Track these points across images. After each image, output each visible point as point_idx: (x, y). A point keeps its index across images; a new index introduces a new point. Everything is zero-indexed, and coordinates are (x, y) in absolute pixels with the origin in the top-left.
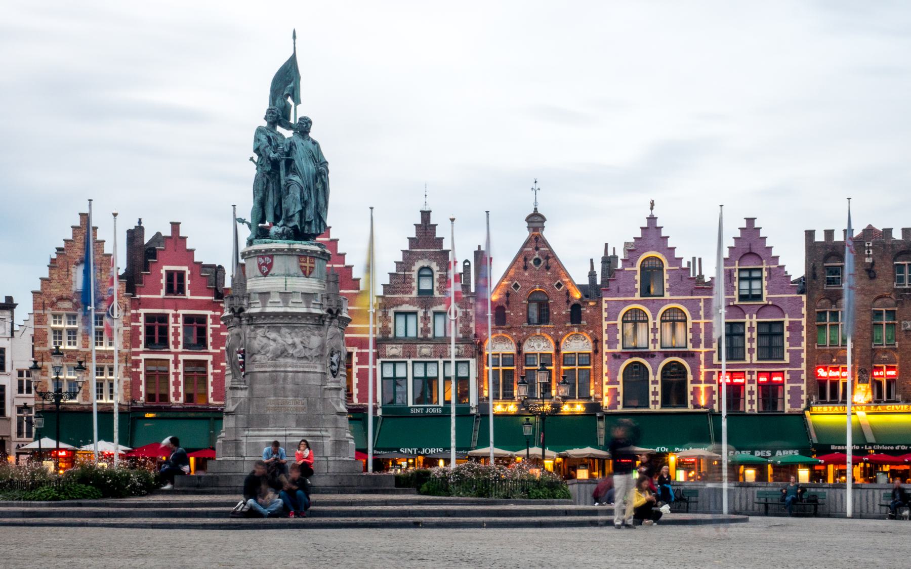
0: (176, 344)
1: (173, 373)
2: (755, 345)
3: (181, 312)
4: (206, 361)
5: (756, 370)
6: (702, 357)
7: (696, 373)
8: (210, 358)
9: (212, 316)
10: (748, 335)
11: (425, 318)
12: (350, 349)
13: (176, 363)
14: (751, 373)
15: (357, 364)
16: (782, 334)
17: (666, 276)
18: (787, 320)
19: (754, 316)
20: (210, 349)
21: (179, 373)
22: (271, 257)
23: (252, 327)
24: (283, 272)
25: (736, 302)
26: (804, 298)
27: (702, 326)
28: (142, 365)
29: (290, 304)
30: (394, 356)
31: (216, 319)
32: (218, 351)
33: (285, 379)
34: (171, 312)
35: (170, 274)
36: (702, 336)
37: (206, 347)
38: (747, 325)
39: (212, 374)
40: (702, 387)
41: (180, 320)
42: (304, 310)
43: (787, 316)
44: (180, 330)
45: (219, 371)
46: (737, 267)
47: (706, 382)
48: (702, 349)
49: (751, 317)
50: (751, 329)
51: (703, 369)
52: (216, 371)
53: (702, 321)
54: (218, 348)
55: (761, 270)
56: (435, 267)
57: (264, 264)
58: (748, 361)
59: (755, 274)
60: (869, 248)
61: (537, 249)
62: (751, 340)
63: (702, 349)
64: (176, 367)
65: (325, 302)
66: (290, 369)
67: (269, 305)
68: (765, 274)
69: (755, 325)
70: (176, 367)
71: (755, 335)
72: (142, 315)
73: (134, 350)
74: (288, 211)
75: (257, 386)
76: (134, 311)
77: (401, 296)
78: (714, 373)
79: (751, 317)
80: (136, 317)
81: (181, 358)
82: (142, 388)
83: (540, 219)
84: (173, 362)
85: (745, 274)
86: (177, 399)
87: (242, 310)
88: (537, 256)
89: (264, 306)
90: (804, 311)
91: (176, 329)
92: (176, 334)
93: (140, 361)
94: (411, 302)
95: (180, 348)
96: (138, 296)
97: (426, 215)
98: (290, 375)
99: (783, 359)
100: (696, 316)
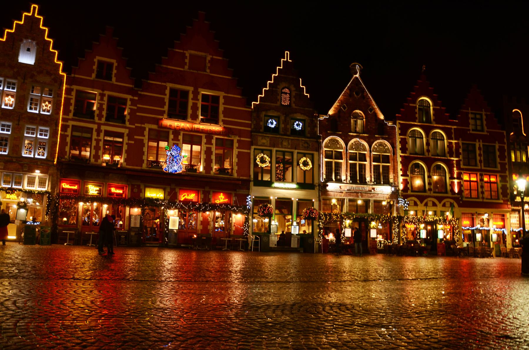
0: (100, 116)
1: (95, 140)
2: (482, 158)
3: (107, 93)
8: (126, 131)
9: (131, 100)
10: (478, 152)
13: (99, 131)
16: (494, 153)
18: (497, 146)
19: (481, 141)
20: (127, 124)
21: (100, 140)
31: (133, 102)
32: (134, 127)
35: (100, 63)
39: (127, 144)
40: (456, 181)
41: (106, 99)
44: (105, 107)
45: (133, 142)
47: (457, 178)
49: (479, 141)
52: (130, 142)
54: (134, 125)
55: (481, 115)
58: (479, 168)
64: (98, 135)
68: (484, 117)
69: (481, 146)
70: (98, 135)
72: (75, 90)
81: (103, 128)
84: (96, 130)
90: (505, 141)
93: (68, 126)
95: (103, 120)
99: (496, 167)
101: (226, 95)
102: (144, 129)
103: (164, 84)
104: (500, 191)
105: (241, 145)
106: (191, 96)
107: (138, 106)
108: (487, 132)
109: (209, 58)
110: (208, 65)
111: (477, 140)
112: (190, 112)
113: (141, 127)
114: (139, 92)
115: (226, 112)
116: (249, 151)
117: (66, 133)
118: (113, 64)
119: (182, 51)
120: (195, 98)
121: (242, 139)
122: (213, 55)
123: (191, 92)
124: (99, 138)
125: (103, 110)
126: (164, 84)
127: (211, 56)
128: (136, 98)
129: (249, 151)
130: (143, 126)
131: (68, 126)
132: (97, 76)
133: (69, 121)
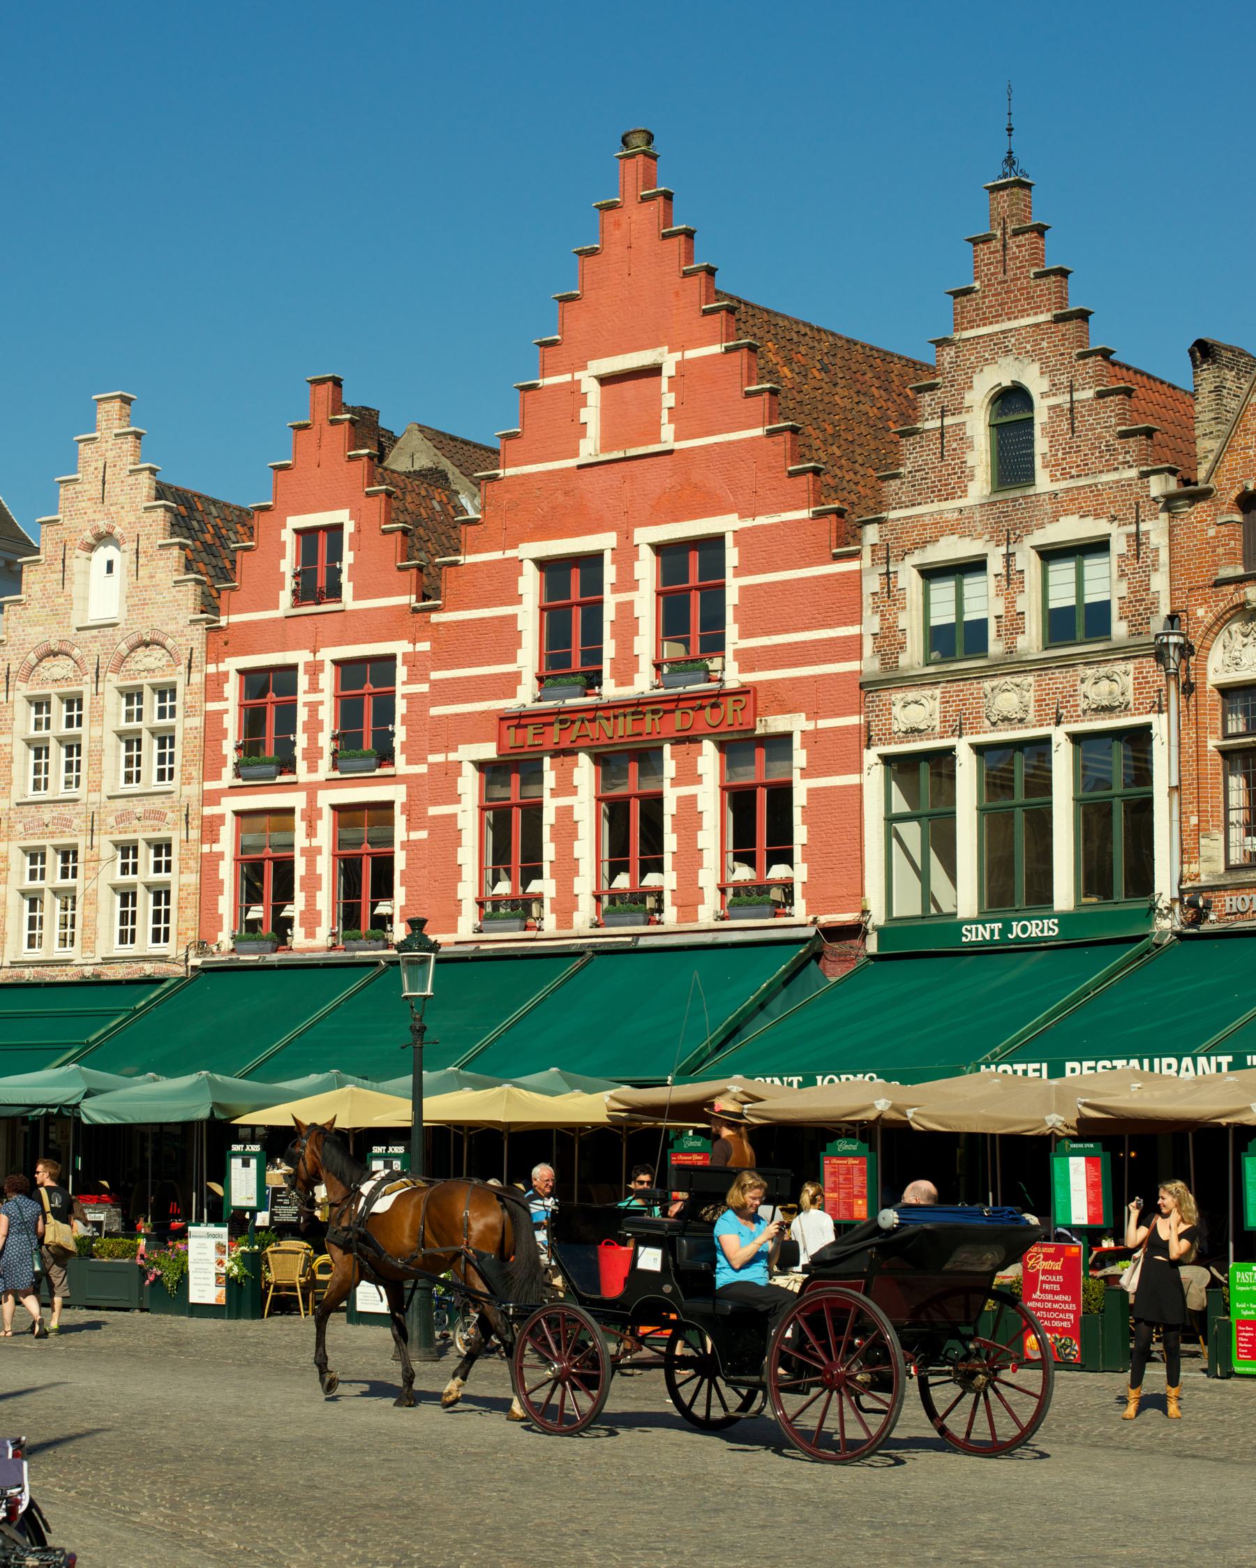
0: (313, 755)
4: (389, 805)
9: (410, 659)
11: (1011, 578)
20: (401, 764)
21: (318, 850)
28: (227, 833)
30: (914, 732)
32: (422, 769)
39: (404, 845)
41: (328, 679)
45: (423, 835)
52: (415, 835)
54: (423, 760)
56: (1036, 383)
64: (311, 832)
70: (311, 832)
73: (209, 785)
76: (212, 669)
77: (935, 507)
80: (214, 687)
82: (226, 904)
86: (310, 934)
91: (313, 707)
92: (314, 726)
93: (221, 818)
94: (960, 527)
95: (325, 769)
96: (223, 621)
101: (748, 523)
103: (510, 553)
106: (610, 573)
107: (435, 675)
109: (669, 370)
110: (669, 400)
113: (447, 763)
114: (435, 618)
116: (852, 779)
117: (216, 848)
118: (339, 527)
119: (567, 378)
120: (627, 583)
121: (824, 723)
122: (683, 348)
124: (315, 842)
126: (510, 553)
127: (677, 356)
128: (424, 646)
129: (852, 779)
130: (453, 757)
132: (300, 597)
133: (223, 800)
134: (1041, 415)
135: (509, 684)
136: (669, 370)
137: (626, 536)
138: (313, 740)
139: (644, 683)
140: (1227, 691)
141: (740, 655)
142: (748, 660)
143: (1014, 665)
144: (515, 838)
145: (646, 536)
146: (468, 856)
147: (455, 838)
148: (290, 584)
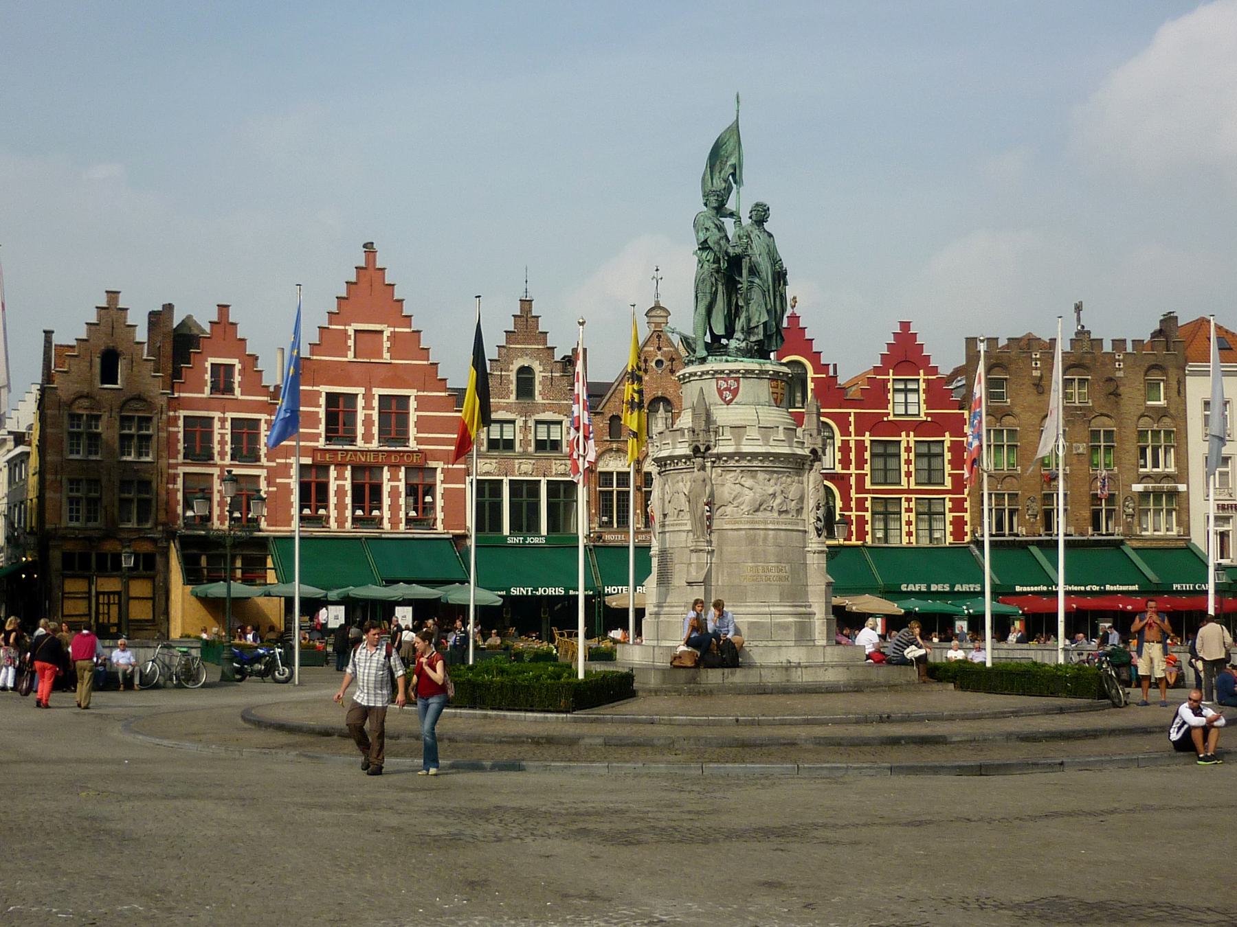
0: (222, 454)
2: (912, 468)
3: (230, 415)
4: (259, 476)
5: (913, 496)
6: (853, 481)
7: (846, 499)
8: (263, 473)
9: (266, 421)
10: (904, 456)
11: (525, 427)
12: (432, 464)
14: (908, 500)
15: (442, 482)
17: (810, 385)
19: (912, 434)
20: (264, 461)
22: (737, 380)
23: (719, 470)
24: (751, 400)
25: (891, 418)
26: (966, 413)
27: (852, 444)
28: (180, 481)
29: (772, 443)
33: (765, 539)
34: (217, 415)
36: (852, 456)
37: (258, 460)
38: (903, 445)
41: (228, 425)
42: (786, 450)
43: (947, 434)
44: (228, 438)
46: (891, 377)
48: (853, 470)
49: (908, 435)
50: (908, 449)
51: (853, 494)
53: (852, 439)
56: (537, 367)
57: (728, 389)
59: (910, 386)
60: (1036, 359)
61: (659, 349)
62: (908, 462)
63: (853, 470)
65: (807, 440)
66: (771, 526)
67: (744, 442)
68: (923, 386)
69: (912, 444)
71: (912, 456)
73: (171, 461)
74: (749, 320)
75: (728, 549)
78: (866, 499)
79: (908, 435)
83: (663, 314)
85: (902, 386)
87: (708, 448)
88: (659, 357)
89: (738, 444)
91: (223, 435)
94: (507, 408)
95: (228, 460)
96: (176, 395)
97: (526, 303)
98: (771, 532)
100: (845, 432)
102: (289, 466)
104: (949, 528)
105: (449, 476)
106: (360, 402)
108: (926, 415)
109: (386, 334)
110: (387, 344)
111: (903, 434)
112: (360, 430)
115: (422, 424)
116: (462, 486)
123: (360, 397)
125: (226, 443)
129: (462, 486)
131: (177, 475)
134: (538, 378)
135: (315, 437)
136: (386, 334)
137: (368, 390)
138: (223, 447)
139: (374, 445)
140: (600, 473)
141: (416, 439)
142: (419, 441)
143: (525, 455)
144: (314, 493)
145: (377, 392)
146: (295, 498)
147: (290, 492)
148: (209, 384)
